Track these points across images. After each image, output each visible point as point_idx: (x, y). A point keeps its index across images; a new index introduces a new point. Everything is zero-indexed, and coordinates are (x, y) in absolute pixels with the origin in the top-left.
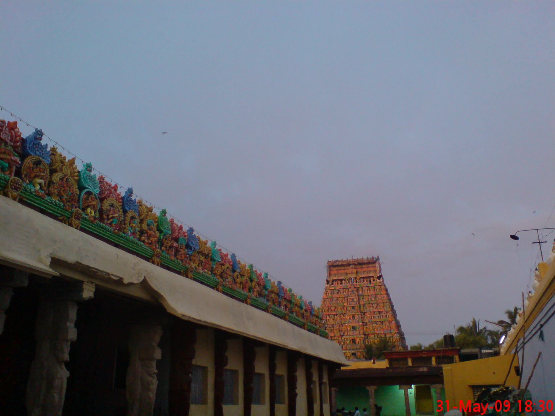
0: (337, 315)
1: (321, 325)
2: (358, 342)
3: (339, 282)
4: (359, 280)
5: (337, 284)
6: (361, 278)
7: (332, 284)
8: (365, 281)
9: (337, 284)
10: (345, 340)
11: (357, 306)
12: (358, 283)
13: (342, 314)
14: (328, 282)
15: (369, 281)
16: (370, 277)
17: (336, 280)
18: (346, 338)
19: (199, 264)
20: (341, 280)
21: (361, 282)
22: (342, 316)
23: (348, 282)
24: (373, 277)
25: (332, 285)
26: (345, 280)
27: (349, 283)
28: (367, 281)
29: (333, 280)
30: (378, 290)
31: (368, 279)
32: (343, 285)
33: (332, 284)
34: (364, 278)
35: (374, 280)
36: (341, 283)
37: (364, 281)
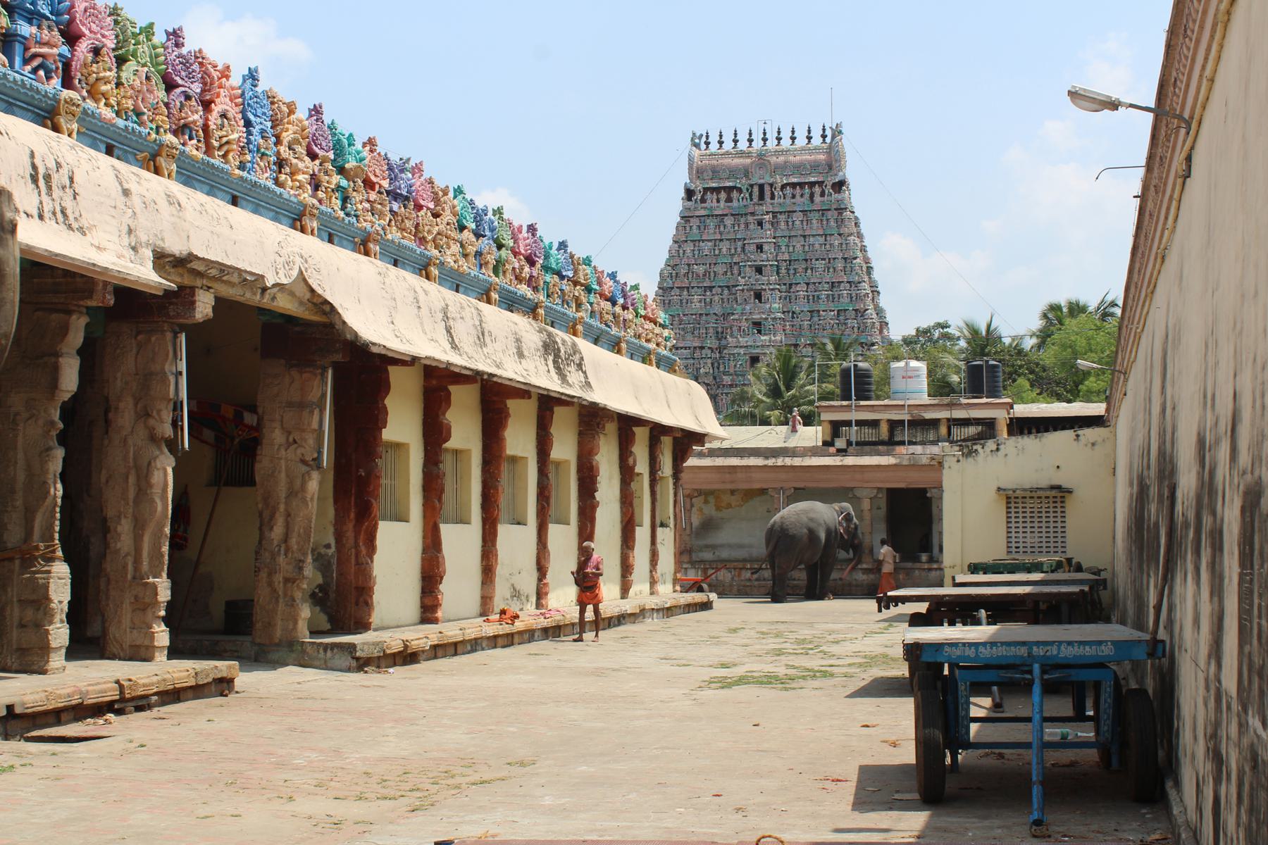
0: (711, 288)
1: (660, 340)
3: (723, 195)
4: (781, 193)
5: (715, 201)
6: (783, 187)
7: (703, 200)
8: (798, 196)
9: (718, 201)
10: (729, 360)
11: (771, 265)
12: (776, 201)
13: (728, 287)
14: (689, 193)
15: (807, 196)
16: (812, 184)
17: (713, 190)
18: (733, 354)
19: (390, 220)
20: (729, 190)
21: (784, 198)
22: (726, 292)
23: (747, 195)
24: (820, 183)
25: (703, 205)
26: (740, 190)
27: (751, 200)
28: (802, 196)
29: (706, 190)
30: (832, 223)
31: (807, 190)
32: (735, 204)
33: (703, 200)
34: (794, 185)
35: (822, 194)
36: (729, 200)
37: (794, 196)
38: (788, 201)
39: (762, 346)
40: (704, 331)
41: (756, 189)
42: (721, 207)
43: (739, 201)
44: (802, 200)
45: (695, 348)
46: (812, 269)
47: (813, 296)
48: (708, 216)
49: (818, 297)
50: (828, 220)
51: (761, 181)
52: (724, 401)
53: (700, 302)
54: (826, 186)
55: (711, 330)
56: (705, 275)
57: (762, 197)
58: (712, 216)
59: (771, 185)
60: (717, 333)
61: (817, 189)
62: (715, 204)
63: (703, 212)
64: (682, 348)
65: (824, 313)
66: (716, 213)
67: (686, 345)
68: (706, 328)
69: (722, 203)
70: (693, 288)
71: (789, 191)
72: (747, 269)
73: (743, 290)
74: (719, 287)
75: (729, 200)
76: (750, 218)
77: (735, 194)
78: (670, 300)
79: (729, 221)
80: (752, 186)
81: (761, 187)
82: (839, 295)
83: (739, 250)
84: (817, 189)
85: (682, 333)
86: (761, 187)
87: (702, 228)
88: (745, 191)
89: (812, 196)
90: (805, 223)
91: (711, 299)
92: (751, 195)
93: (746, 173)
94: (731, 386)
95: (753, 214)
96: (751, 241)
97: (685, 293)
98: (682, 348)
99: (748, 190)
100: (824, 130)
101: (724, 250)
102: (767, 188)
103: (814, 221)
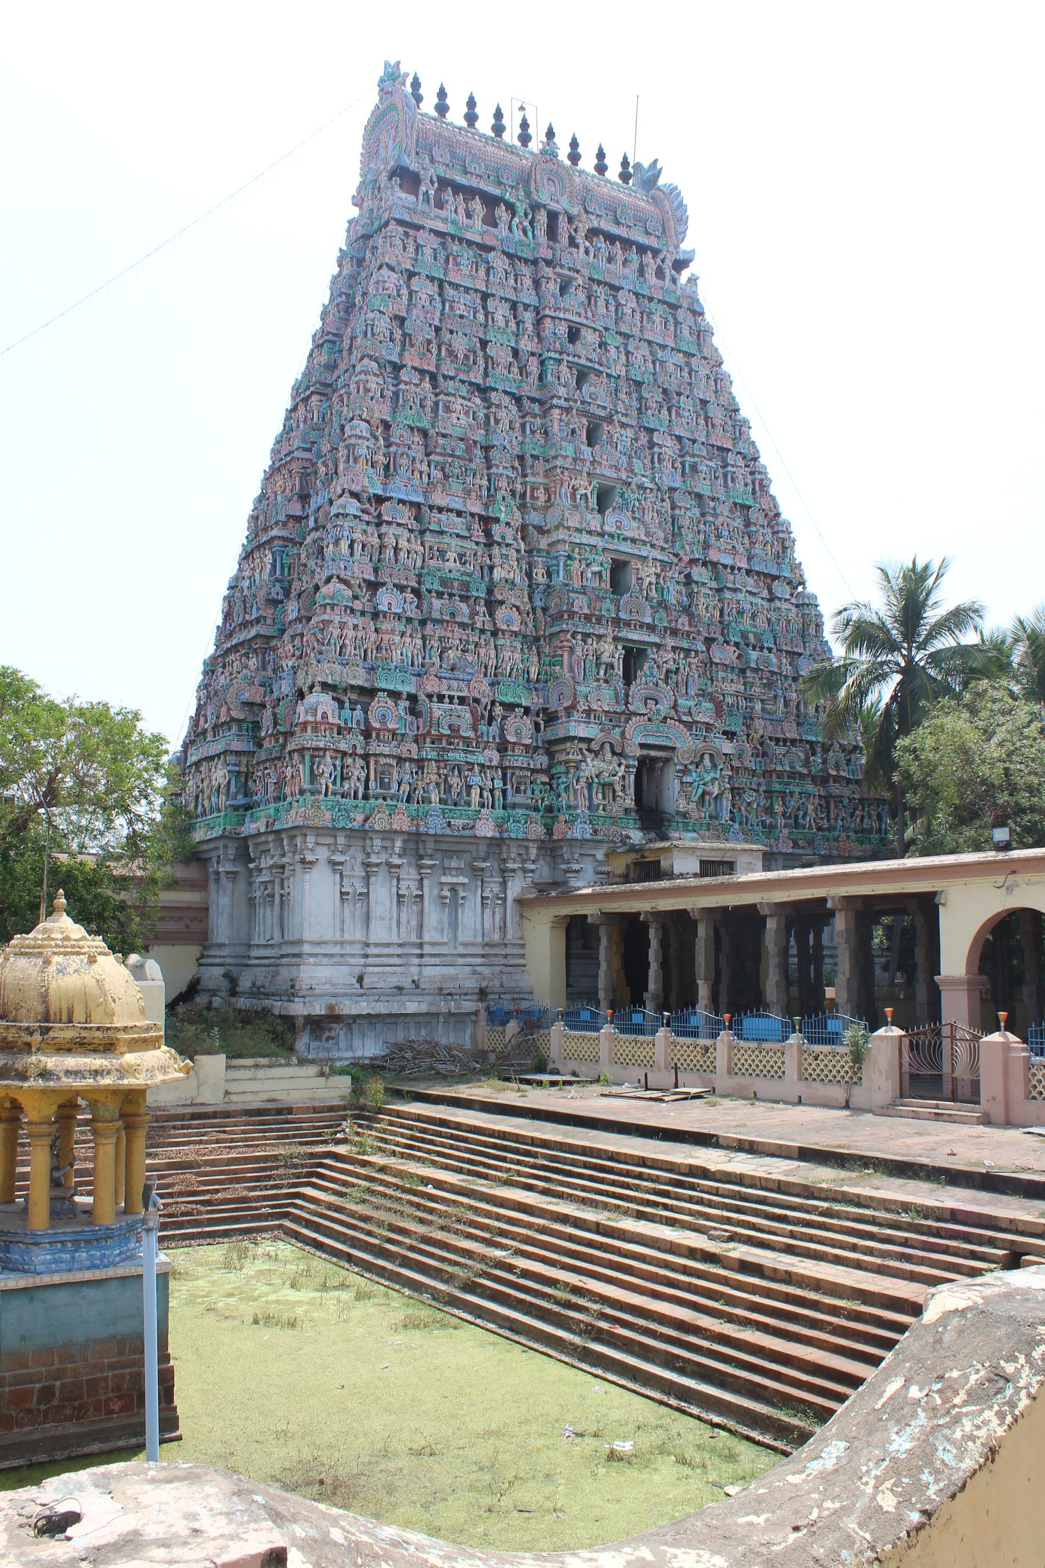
2: (650, 583)
3: (477, 205)
4: (588, 244)
5: (461, 210)
6: (593, 233)
10: (569, 557)
15: (635, 266)
16: (642, 249)
17: (458, 189)
23: (526, 223)
24: (656, 252)
26: (511, 208)
28: (625, 262)
29: (444, 183)
31: (634, 256)
32: (503, 231)
34: (611, 238)
38: (603, 264)
39: (634, 541)
40: (485, 482)
41: (542, 217)
42: (476, 230)
43: (510, 229)
44: (626, 271)
45: (472, 515)
46: (669, 410)
47: (683, 464)
48: (453, 237)
49: (694, 467)
50: (677, 323)
51: (554, 206)
52: (579, 652)
53: (467, 413)
54: (663, 261)
55: (503, 484)
56: (466, 357)
57: (552, 233)
58: (461, 240)
59: (571, 219)
60: (513, 493)
61: (648, 258)
62: (461, 217)
63: (440, 227)
64: (440, 510)
65: (712, 504)
66: (469, 236)
67: (452, 506)
68: (489, 476)
69: (478, 224)
70: (445, 377)
71: (601, 243)
72: (563, 368)
73: (568, 410)
74: (505, 392)
75: (491, 221)
76: (548, 271)
77: (501, 212)
78: (396, 394)
79: (499, 262)
80: (535, 207)
81: (552, 216)
82: (725, 476)
83: (529, 326)
84: (648, 258)
85: (437, 474)
86: (552, 216)
87: (442, 257)
88: (521, 207)
89: (641, 272)
90: (638, 317)
91: (487, 417)
92: (532, 223)
93: (525, 180)
94: (588, 618)
95: (549, 263)
96: (561, 315)
97: (427, 385)
98: (440, 510)
99: (526, 215)
100: (625, 163)
101: (498, 317)
102: (562, 222)
103: (657, 319)
